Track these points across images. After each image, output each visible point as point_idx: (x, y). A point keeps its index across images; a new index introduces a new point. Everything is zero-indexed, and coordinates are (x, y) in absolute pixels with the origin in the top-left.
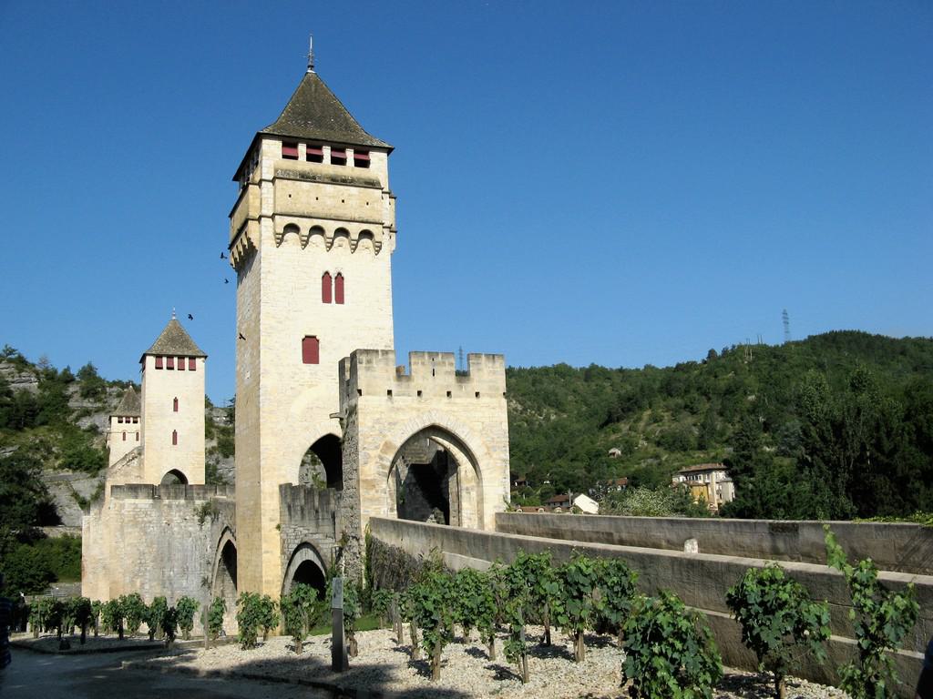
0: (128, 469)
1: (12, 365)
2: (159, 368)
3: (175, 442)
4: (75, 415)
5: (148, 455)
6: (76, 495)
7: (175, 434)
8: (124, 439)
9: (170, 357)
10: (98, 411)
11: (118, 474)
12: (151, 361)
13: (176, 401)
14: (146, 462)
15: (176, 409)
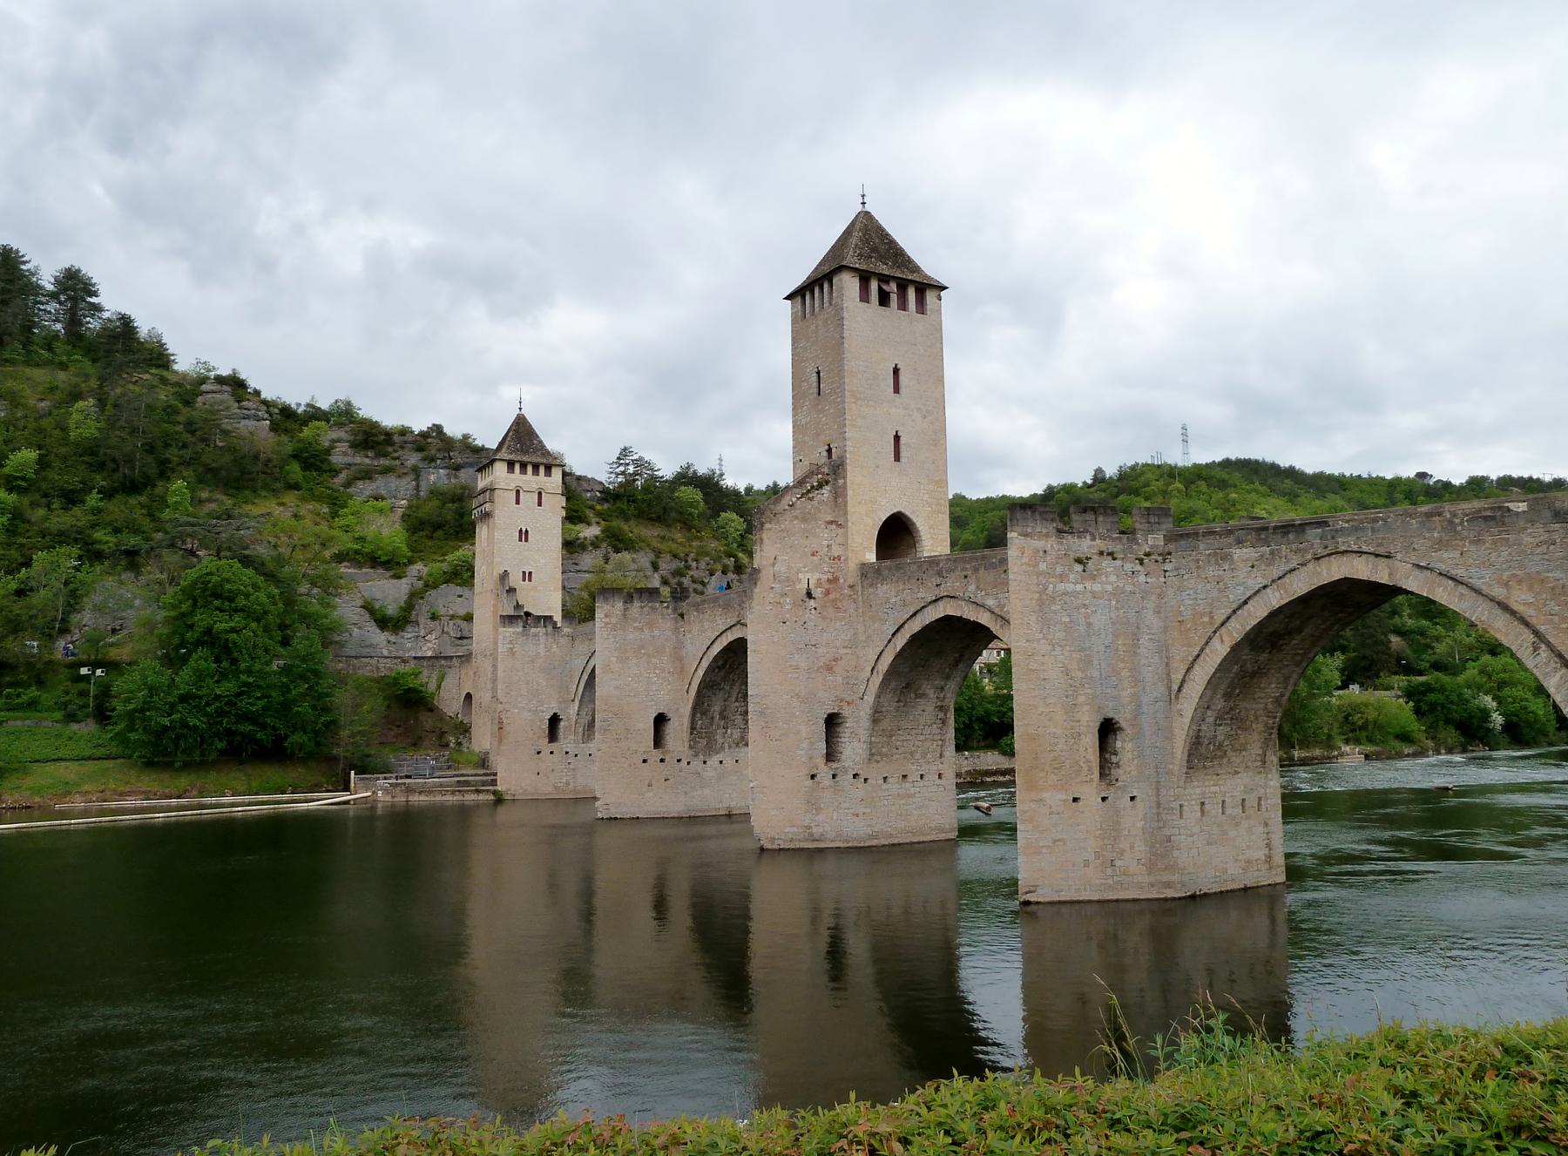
0: (809, 505)
1: (225, 388)
2: (865, 296)
3: (897, 458)
4: (343, 476)
5: (855, 477)
6: (368, 607)
7: (897, 438)
8: (518, 502)
9: (884, 279)
10: (386, 471)
11: (788, 516)
12: (848, 284)
13: (896, 371)
14: (850, 492)
15: (897, 390)
